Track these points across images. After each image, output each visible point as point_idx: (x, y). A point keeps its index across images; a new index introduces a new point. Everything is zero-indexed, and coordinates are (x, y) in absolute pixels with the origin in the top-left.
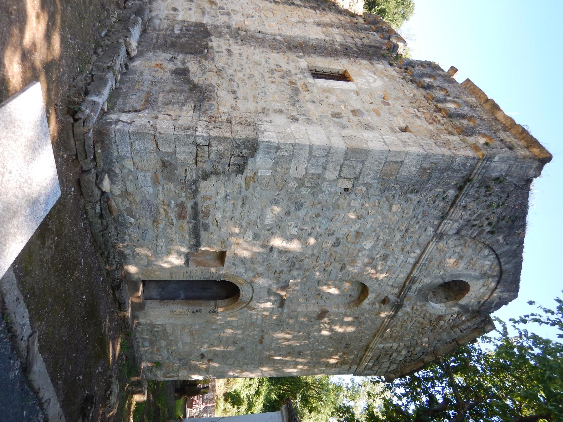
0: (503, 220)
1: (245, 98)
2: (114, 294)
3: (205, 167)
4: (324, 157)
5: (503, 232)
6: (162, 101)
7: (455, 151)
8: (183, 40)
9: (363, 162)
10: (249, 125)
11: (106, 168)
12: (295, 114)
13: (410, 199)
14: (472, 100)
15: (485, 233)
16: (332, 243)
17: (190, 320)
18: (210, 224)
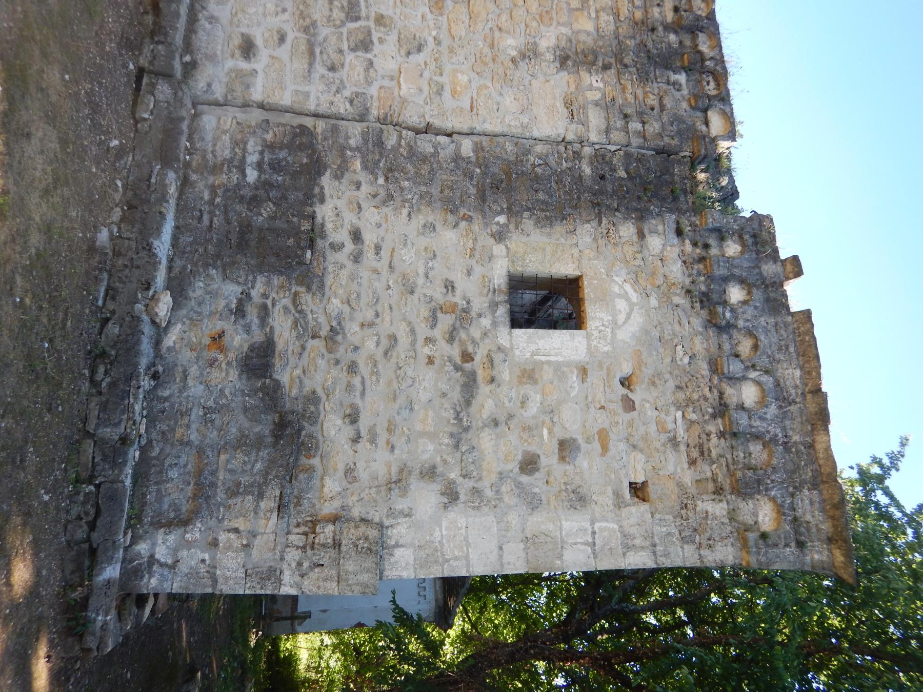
1: (373, 441)
6: (224, 484)
14: (792, 375)
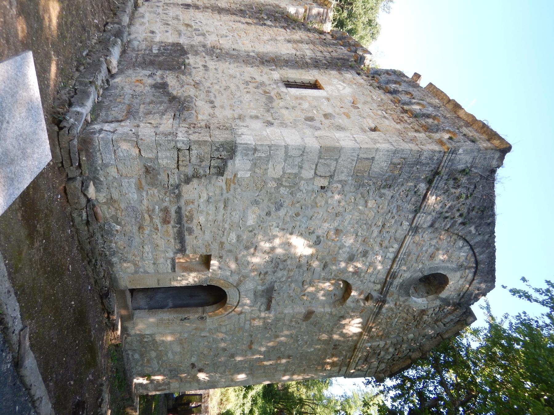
0: (473, 210)
2: (102, 303)
3: (186, 171)
4: (299, 157)
5: (475, 223)
6: (143, 112)
7: (422, 146)
8: (161, 59)
9: (337, 160)
10: (227, 129)
11: (91, 176)
12: (270, 119)
13: (384, 194)
14: (436, 101)
15: (457, 224)
16: (314, 241)
17: (179, 328)
18: (195, 228)
